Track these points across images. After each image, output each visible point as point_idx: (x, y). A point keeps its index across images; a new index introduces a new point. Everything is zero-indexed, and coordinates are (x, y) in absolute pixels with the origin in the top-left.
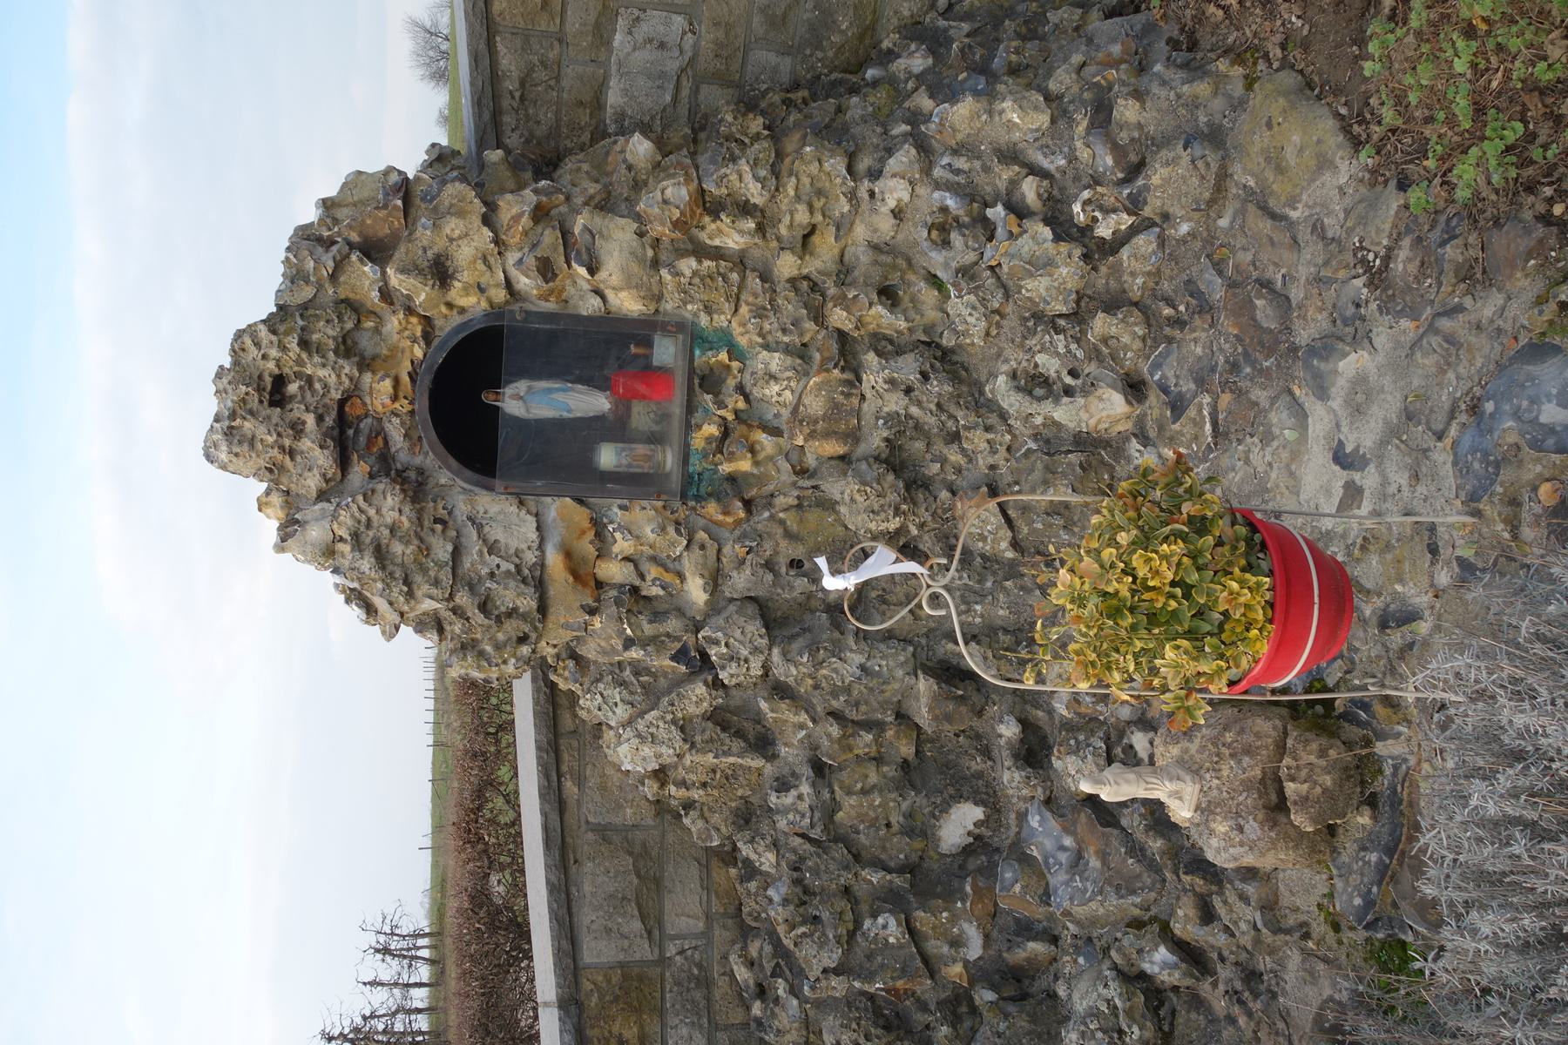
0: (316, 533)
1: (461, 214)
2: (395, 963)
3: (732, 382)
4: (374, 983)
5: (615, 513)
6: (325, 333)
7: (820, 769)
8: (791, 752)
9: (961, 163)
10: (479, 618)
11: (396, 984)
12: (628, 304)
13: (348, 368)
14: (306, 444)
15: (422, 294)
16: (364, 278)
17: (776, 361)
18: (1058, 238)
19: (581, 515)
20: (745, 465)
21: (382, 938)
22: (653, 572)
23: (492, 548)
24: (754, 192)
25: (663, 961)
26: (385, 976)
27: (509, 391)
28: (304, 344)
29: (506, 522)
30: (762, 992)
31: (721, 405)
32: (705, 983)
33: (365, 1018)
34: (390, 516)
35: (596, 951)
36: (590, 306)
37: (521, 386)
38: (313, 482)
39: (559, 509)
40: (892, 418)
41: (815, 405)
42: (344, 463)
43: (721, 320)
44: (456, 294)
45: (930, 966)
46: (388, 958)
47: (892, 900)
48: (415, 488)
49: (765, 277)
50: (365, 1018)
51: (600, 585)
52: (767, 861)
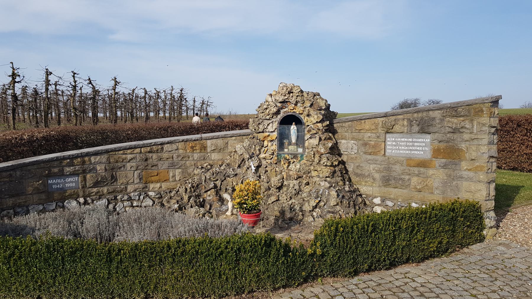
0: (270, 99)
1: (317, 118)
2: (200, 106)
3: (295, 160)
4: (194, 101)
5: (276, 143)
6: (299, 99)
7: (236, 175)
8: (239, 171)
9: (327, 193)
10: (258, 123)
11: (194, 106)
12: (306, 144)
13: (294, 102)
14: (283, 97)
15: (306, 113)
16: (308, 104)
17: (298, 166)
18: (313, 207)
19: (274, 138)
20: (282, 163)
21: (206, 102)
22: (266, 149)
23: (268, 125)
24: (322, 162)
25: (207, 153)
26: (196, 104)
27: (295, 126)
28: (297, 96)
29: (273, 126)
30: (202, 168)
31: (292, 158)
32: (204, 159)
33: (185, 99)
34: (272, 110)
35: (209, 142)
36: (306, 138)
37: (296, 128)
38: (277, 98)
39: (275, 135)
40: (289, 185)
41: (291, 173)
42: (280, 102)
43: (305, 158)
44: (306, 117)
45: (206, 192)
46: (201, 104)
47: (215, 187)
48: (278, 113)
49: (311, 165)
50: (185, 99)
51: (264, 141)
52: (222, 168)
